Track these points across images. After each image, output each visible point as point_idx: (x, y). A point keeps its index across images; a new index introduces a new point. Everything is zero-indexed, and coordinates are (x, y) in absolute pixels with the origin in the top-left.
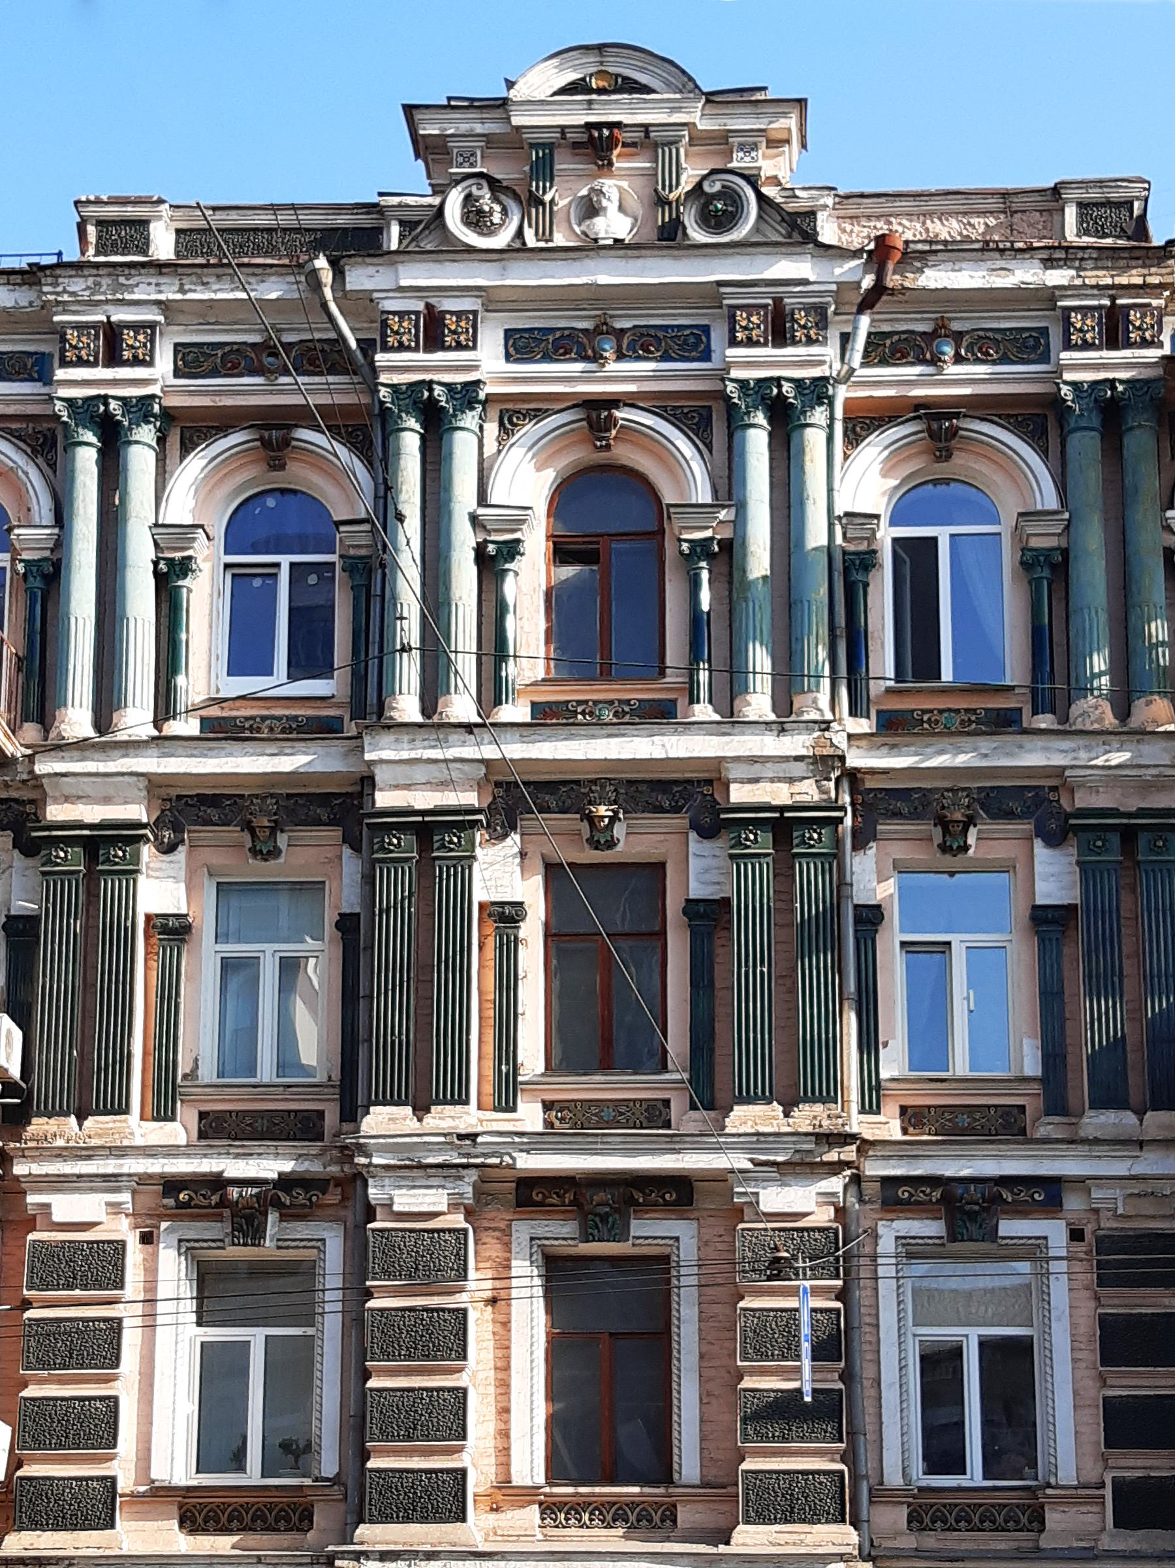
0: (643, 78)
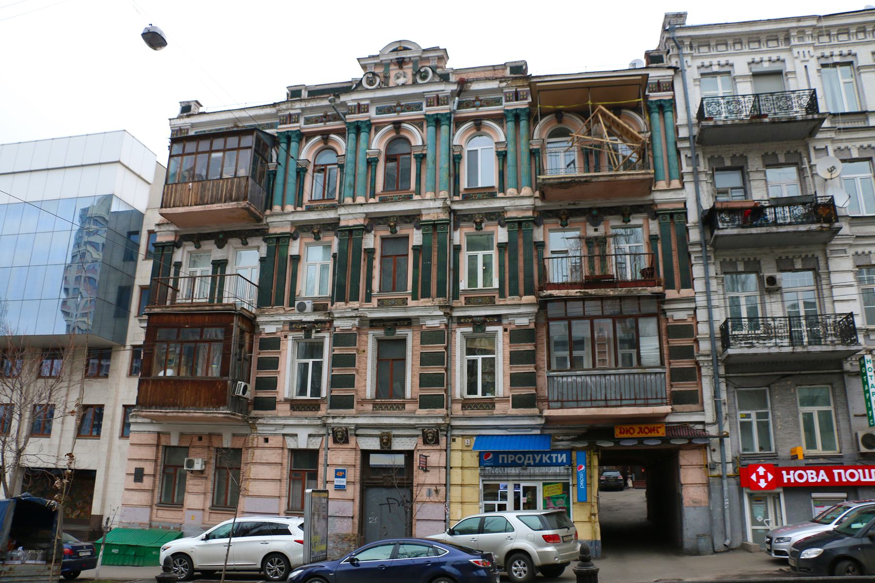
0: (409, 47)
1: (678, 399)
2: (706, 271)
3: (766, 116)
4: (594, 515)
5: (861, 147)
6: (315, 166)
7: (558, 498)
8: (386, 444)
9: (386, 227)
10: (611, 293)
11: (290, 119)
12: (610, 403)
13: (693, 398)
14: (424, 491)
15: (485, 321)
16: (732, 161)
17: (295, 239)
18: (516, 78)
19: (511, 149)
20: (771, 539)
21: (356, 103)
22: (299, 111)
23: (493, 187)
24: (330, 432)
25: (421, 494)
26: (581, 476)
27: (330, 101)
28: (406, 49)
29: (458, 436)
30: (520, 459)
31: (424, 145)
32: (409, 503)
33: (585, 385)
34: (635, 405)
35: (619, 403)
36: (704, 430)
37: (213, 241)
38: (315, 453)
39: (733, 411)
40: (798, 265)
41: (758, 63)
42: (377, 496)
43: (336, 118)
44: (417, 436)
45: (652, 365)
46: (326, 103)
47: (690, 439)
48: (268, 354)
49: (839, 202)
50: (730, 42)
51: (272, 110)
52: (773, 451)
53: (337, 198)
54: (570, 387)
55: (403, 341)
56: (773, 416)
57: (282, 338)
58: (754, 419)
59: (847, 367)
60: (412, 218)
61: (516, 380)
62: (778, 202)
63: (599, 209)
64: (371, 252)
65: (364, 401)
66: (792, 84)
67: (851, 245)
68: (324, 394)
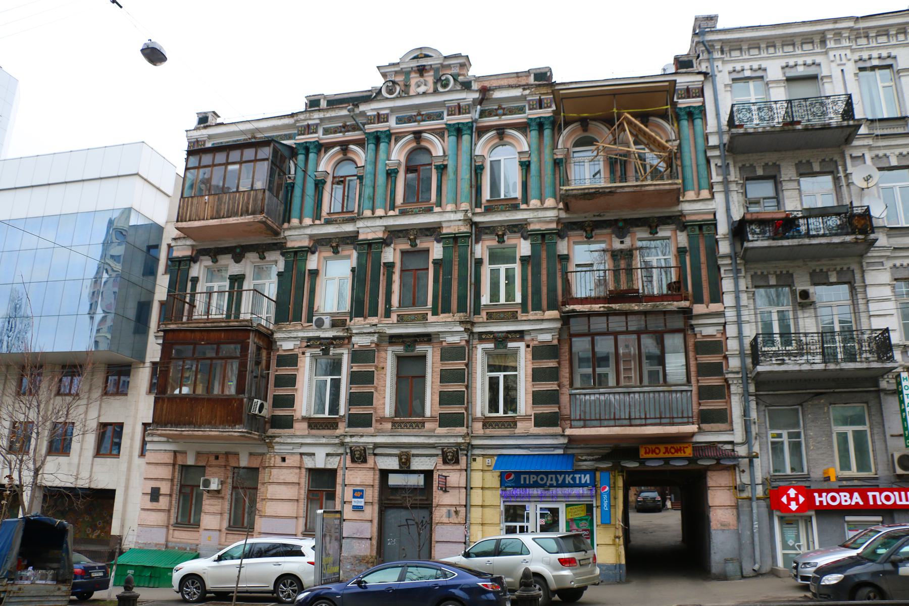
0: (430, 54)
1: (706, 417)
2: (736, 285)
3: (799, 123)
4: (619, 537)
5: (901, 154)
6: (334, 177)
7: (581, 520)
8: (405, 463)
9: (405, 240)
10: (636, 308)
11: (308, 129)
12: (634, 422)
13: (722, 417)
14: (444, 510)
15: (507, 338)
16: (764, 170)
17: (313, 253)
18: (540, 85)
19: (534, 159)
20: (798, 564)
21: (375, 113)
22: (317, 121)
23: (516, 199)
24: (348, 451)
25: (439, 515)
26: (605, 497)
27: (349, 111)
28: (427, 56)
29: (479, 455)
30: (542, 479)
31: (445, 155)
32: (428, 525)
33: (608, 404)
34: (660, 424)
35: (643, 422)
36: (733, 450)
37: (230, 256)
38: (333, 472)
39: (763, 431)
40: (833, 279)
41: (792, 67)
42: (395, 517)
43: (355, 128)
44: (437, 455)
45: (679, 382)
46: (344, 112)
47: (718, 460)
48: (285, 371)
49: (874, 213)
50: (763, 46)
51: (291, 121)
52: (806, 472)
53: (356, 211)
54: (593, 405)
55: (423, 358)
56: (805, 435)
57: (300, 355)
58: (785, 439)
59: (883, 384)
60: (433, 231)
61: (538, 398)
62: (811, 213)
63: (625, 221)
64: (390, 266)
65: (382, 420)
66: (828, 89)
67: (888, 257)
68: (342, 412)
